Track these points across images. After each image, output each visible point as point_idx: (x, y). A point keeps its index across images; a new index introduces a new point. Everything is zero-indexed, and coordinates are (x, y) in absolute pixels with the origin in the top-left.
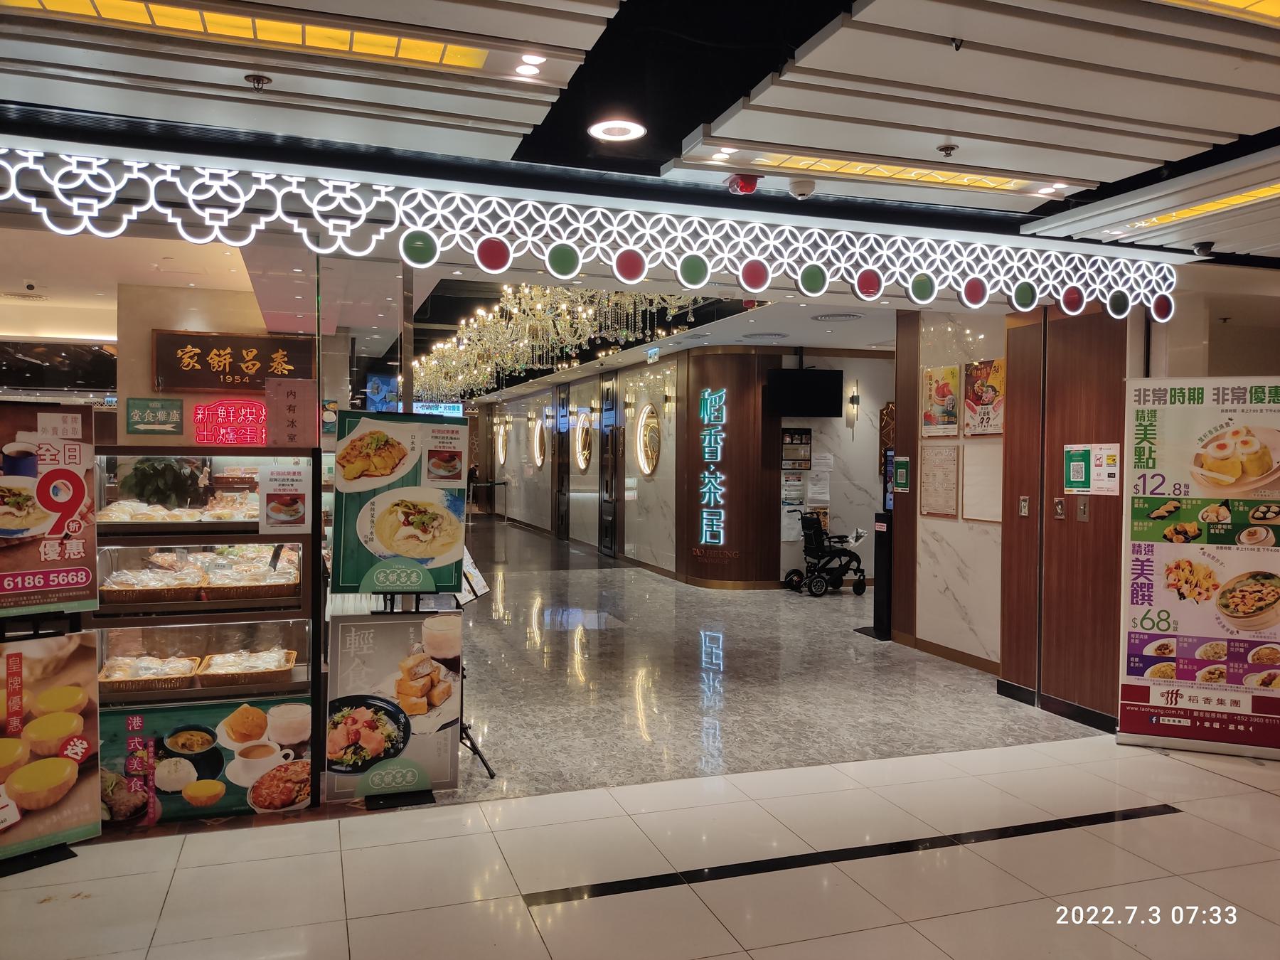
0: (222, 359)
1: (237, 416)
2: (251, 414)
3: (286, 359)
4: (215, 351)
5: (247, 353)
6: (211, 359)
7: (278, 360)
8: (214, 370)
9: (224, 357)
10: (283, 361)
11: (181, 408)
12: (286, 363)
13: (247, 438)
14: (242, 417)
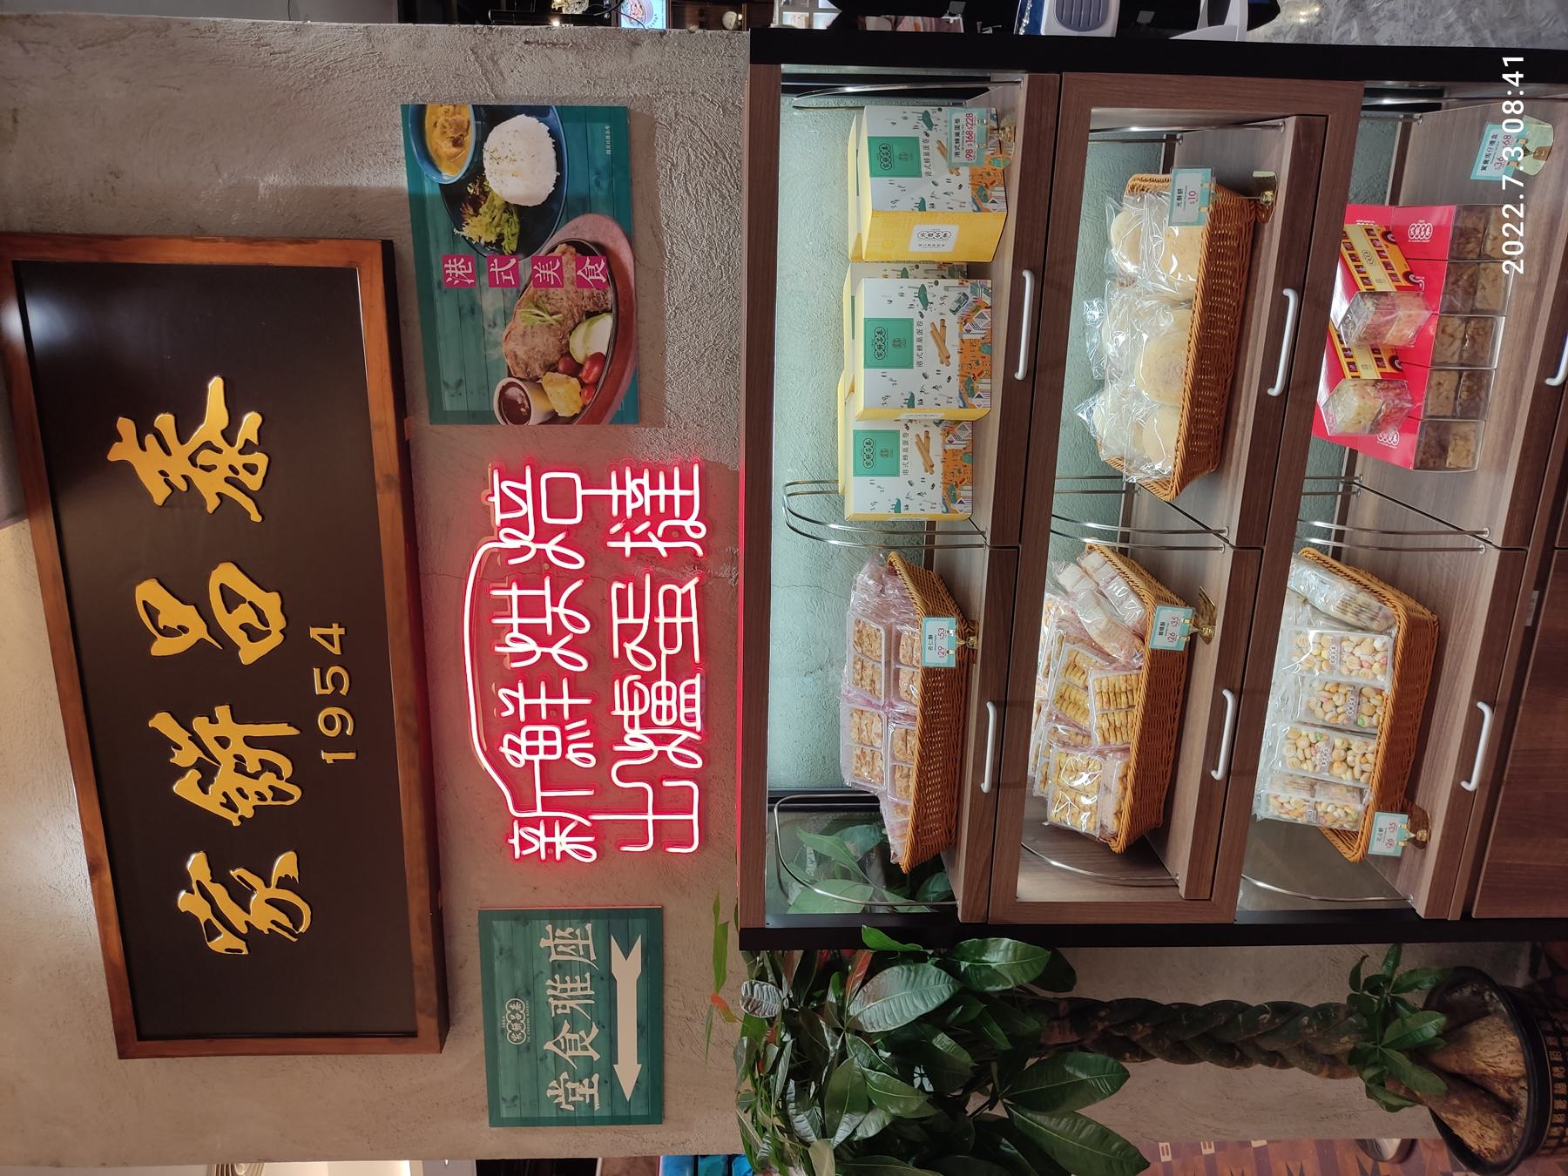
0: (225, 758)
1: (542, 676)
2: (531, 607)
3: (165, 422)
4: (186, 788)
5: (167, 632)
6: (230, 805)
7: (178, 466)
8: (296, 792)
9: (214, 748)
10: (183, 438)
11: (523, 917)
12: (189, 420)
13: (670, 628)
14: (555, 651)
